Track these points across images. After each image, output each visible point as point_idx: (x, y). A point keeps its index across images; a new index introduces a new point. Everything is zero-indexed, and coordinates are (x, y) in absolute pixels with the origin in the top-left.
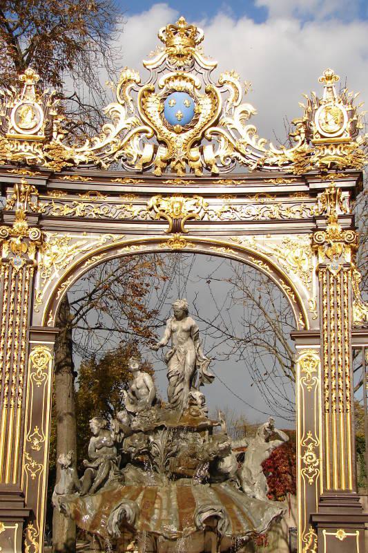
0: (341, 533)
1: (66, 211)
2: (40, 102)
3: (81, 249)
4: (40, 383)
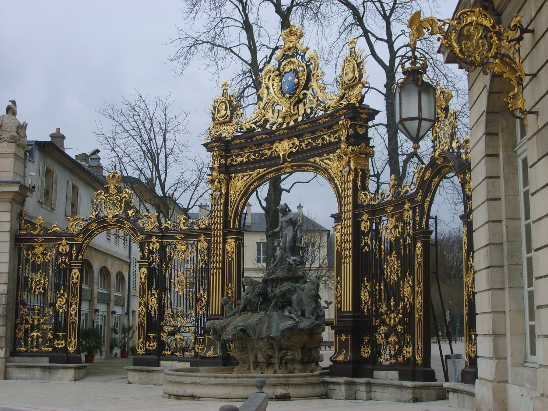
1: (239, 160)
2: (229, 99)
3: (246, 182)
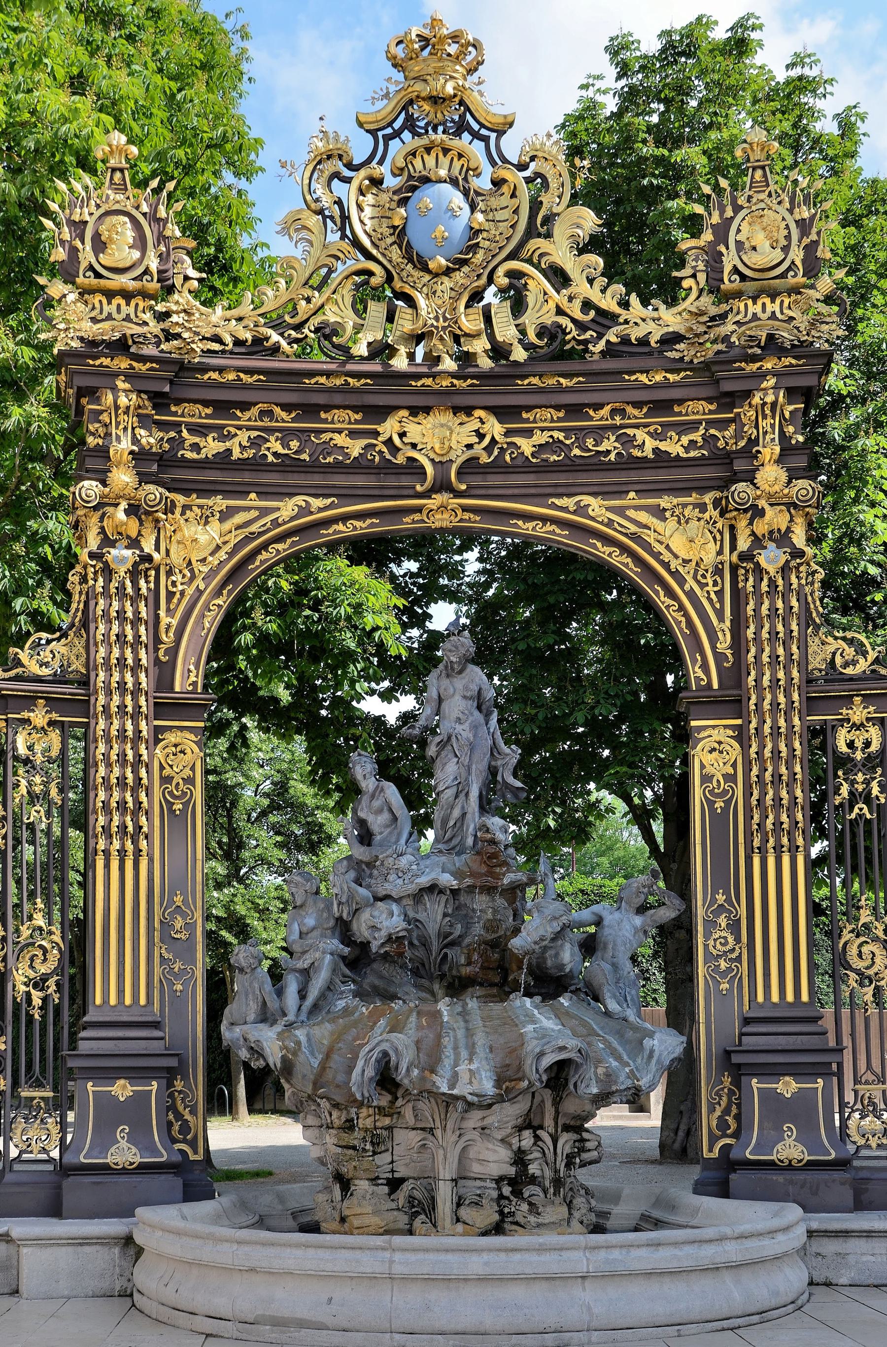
0: (787, 1084)
1: (212, 446)
4: (180, 806)
